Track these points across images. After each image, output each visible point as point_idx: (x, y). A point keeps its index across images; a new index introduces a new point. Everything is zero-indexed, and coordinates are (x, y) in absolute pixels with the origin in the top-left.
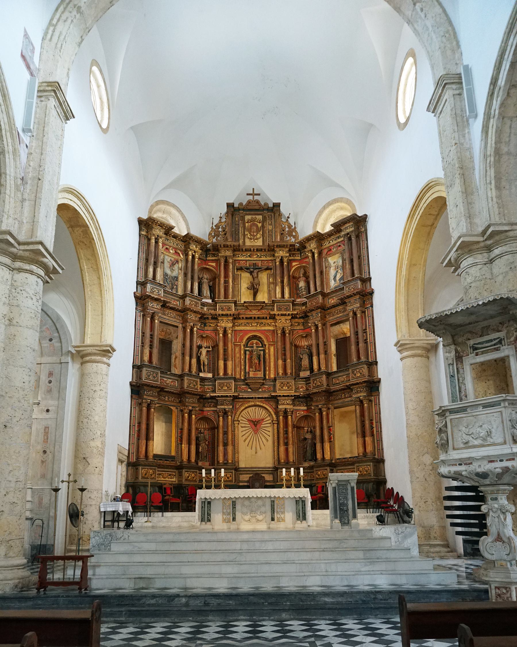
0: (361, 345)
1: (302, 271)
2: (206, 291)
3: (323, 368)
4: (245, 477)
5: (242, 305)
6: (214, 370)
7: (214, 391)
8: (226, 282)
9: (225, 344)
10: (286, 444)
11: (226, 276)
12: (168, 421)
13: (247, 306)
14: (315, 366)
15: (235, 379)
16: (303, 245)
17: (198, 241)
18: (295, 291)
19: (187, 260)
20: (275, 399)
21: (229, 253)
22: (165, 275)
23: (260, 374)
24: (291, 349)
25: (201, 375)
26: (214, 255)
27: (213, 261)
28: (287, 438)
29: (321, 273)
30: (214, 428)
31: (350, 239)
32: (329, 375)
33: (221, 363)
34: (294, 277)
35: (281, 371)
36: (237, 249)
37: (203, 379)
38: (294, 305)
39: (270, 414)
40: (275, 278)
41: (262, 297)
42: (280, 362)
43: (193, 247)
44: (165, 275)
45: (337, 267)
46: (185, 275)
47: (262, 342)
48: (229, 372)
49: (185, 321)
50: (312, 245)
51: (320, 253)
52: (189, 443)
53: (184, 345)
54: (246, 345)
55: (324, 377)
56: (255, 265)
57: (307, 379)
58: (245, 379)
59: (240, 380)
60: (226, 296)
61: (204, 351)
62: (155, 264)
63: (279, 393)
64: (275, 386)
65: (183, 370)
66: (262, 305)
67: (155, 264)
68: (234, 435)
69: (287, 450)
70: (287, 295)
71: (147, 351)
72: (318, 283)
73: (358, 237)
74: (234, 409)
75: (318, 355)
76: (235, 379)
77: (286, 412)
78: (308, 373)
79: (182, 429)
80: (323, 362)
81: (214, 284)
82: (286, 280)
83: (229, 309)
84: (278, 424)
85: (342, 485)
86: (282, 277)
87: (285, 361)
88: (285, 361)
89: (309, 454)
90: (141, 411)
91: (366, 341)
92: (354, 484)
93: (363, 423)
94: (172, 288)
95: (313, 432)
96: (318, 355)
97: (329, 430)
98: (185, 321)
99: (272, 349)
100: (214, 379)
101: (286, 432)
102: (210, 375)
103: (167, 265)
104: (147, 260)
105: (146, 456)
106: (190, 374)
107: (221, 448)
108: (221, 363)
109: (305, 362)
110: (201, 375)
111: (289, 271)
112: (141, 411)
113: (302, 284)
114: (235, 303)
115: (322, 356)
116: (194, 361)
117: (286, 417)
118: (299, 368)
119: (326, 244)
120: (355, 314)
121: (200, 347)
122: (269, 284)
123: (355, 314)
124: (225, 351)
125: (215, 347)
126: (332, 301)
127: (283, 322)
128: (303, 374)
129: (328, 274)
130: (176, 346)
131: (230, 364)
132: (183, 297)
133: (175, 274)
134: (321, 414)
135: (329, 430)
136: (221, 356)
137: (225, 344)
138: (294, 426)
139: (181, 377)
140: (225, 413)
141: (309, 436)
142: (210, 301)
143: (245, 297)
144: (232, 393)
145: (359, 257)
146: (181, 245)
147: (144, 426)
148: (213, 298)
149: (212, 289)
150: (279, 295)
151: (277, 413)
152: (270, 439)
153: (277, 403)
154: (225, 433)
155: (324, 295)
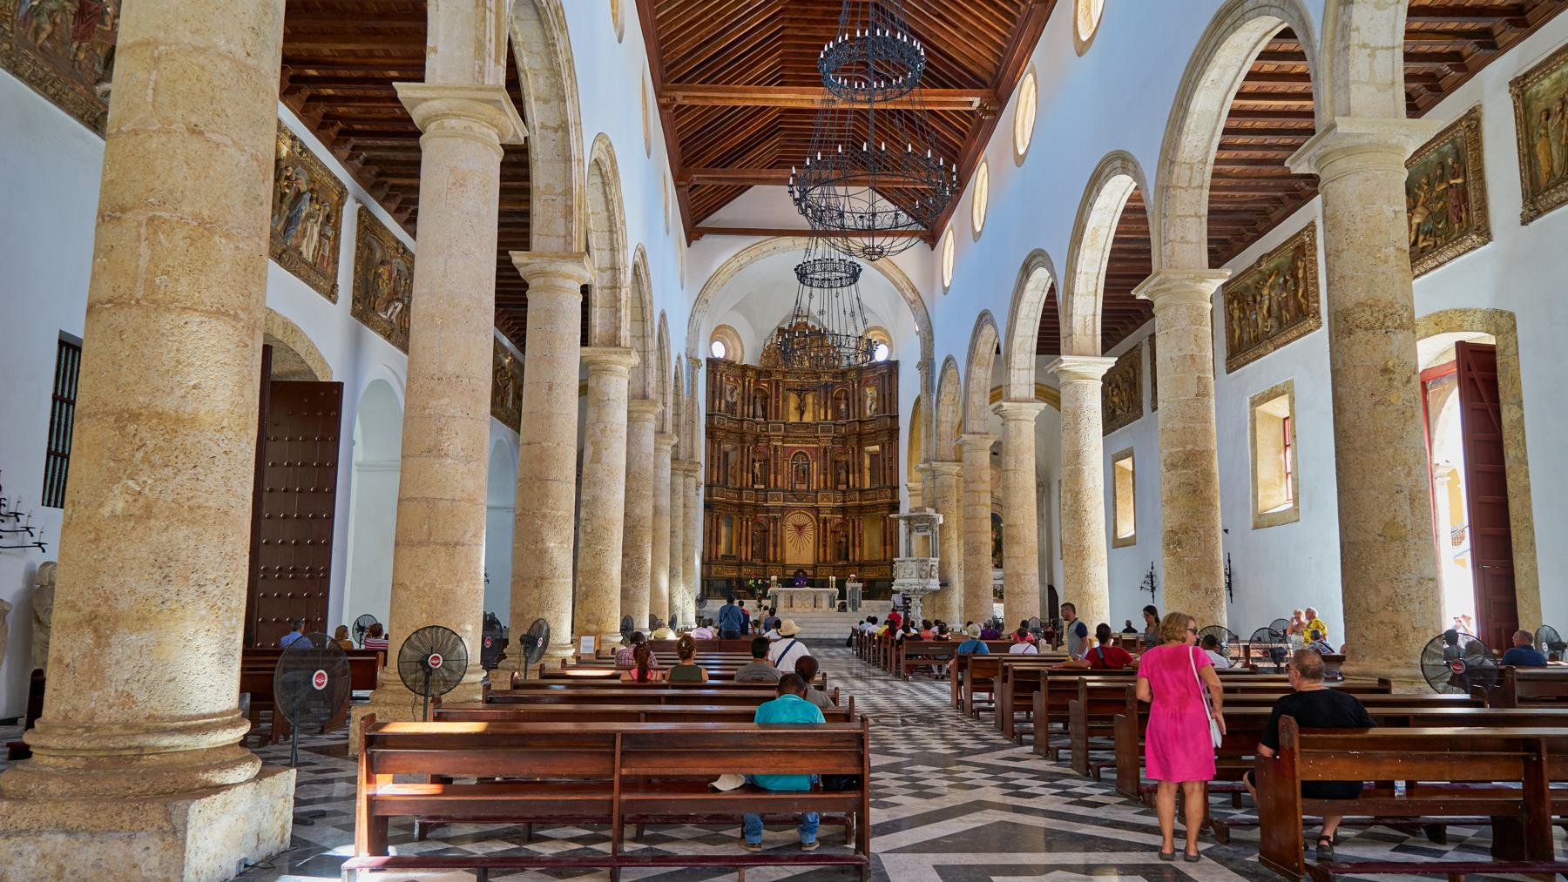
0: (887, 472)
1: (844, 394)
2: (759, 412)
3: (857, 485)
4: (791, 572)
5: (791, 424)
6: (766, 481)
7: (766, 501)
8: (777, 402)
9: (776, 459)
10: (825, 546)
11: (777, 396)
12: (730, 525)
13: (795, 425)
14: (851, 483)
15: (784, 491)
16: (844, 373)
17: (753, 369)
18: (836, 411)
19: (744, 384)
20: (817, 510)
21: (779, 377)
22: (727, 402)
23: (804, 487)
24: (831, 465)
25: (756, 486)
26: (766, 376)
27: (764, 382)
28: (825, 541)
29: (860, 400)
30: (766, 531)
31: (883, 377)
32: (861, 491)
33: (772, 476)
34: (836, 399)
35: (822, 485)
36: (784, 374)
37: (757, 490)
38: (834, 424)
39: (812, 521)
40: (819, 401)
41: (808, 418)
42: (822, 477)
43: (750, 373)
44: (727, 402)
45: (872, 399)
46: (743, 399)
47: (807, 457)
48: (779, 484)
49: (742, 441)
50: (853, 375)
51: (859, 382)
52: (747, 545)
53: (742, 462)
54: (793, 460)
55: (857, 494)
56: (802, 386)
57: (844, 492)
58: (792, 491)
59: (787, 491)
60: (777, 417)
61: (757, 465)
62: (720, 394)
63: (820, 504)
64: (816, 496)
65: (741, 484)
66: (807, 425)
67: (720, 394)
68: (782, 538)
69: (825, 551)
70: (829, 418)
71: (715, 472)
72: (856, 411)
73: (890, 376)
74: (783, 516)
75: (854, 473)
76: (784, 491)
77: (825, 519)
78: (844, 487)
79: (741, 533)
80: (857, 480)
81: (766, 403)
82: (829, 403)
83: (780, 430)
84: (819, 529)
85: (854, 589)
86: (826, 398)
87: (825, 475)
88: (825, 475)
89: (843, 555)
90: (712, 520)
91: (891, 468)
92: (860, 589)
93: (885, 533)
94: (732, 414)
95: (847, 537)
96: (854, 473)
97: (860, 537)
98: (742, 441)
99: (815, 464)
100: (766, 490)
101: (825, 536)
102: (762, 487)
103: (728, 393)
104: (713, 392)
105: (717, 557)
106: (747, 488)
107: (771, 549)
108: (772, 476)
109: (843, 477)
110: (756, 486)
111: (832, 393)
112: (712, 520)
113: (843, 407)
114: (784, 423)
115: (857, 475)
116: (750, 476)
117: (825, 524)
118: (837, 482)
119: (865, 375)
120: (883, 444)
121: (754, 461)
122: (814, 405)
123: (883, 444)
124: (776, 464)
125: (767, 461)
126: (868, 428)
127: (825, 443)
128: (840, 487)
129: (865, 403)
130: (733, 457)
131: (779, 477)
132: (742, 421)
133: (734, 400)
134: (854, 523)
135: (860, 537)
136: (772, 471)
137: (776, 459)
138: (831, 532)
139: (740, 490)
140: (775, 518)
141: (843, 540)
142: (762, 419)
143: (793, 418)
144: (780, 503)
145: (890, 395)
146: (738, 372)
147: (714, 534)
148: (766, 419)
149: (764, 408)
150: (822, 417)
151: (818, 521)
152: (812, 541)
153: (818, 512)
154: (775, 536)
155: (860, 422)
